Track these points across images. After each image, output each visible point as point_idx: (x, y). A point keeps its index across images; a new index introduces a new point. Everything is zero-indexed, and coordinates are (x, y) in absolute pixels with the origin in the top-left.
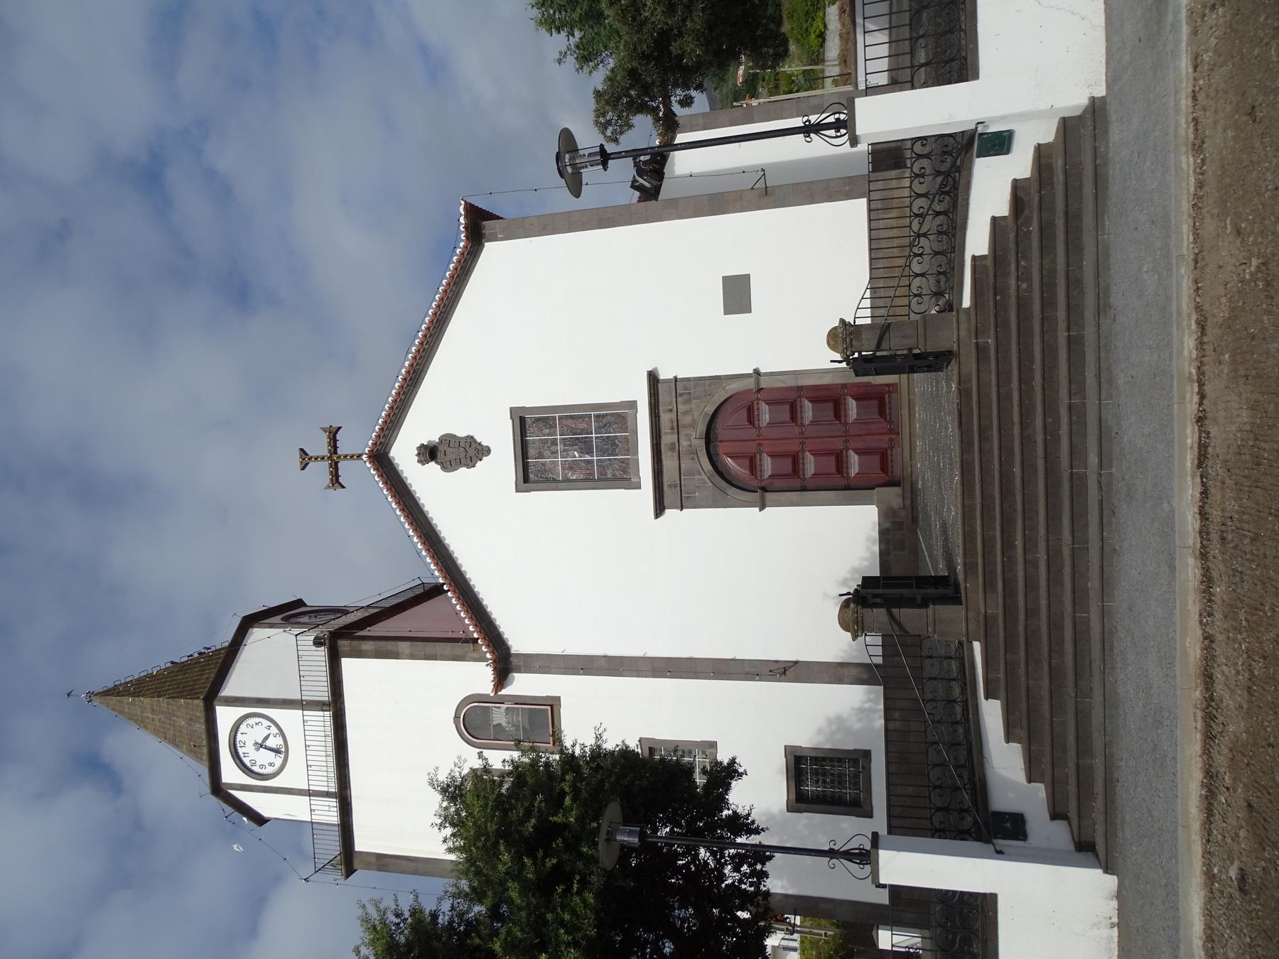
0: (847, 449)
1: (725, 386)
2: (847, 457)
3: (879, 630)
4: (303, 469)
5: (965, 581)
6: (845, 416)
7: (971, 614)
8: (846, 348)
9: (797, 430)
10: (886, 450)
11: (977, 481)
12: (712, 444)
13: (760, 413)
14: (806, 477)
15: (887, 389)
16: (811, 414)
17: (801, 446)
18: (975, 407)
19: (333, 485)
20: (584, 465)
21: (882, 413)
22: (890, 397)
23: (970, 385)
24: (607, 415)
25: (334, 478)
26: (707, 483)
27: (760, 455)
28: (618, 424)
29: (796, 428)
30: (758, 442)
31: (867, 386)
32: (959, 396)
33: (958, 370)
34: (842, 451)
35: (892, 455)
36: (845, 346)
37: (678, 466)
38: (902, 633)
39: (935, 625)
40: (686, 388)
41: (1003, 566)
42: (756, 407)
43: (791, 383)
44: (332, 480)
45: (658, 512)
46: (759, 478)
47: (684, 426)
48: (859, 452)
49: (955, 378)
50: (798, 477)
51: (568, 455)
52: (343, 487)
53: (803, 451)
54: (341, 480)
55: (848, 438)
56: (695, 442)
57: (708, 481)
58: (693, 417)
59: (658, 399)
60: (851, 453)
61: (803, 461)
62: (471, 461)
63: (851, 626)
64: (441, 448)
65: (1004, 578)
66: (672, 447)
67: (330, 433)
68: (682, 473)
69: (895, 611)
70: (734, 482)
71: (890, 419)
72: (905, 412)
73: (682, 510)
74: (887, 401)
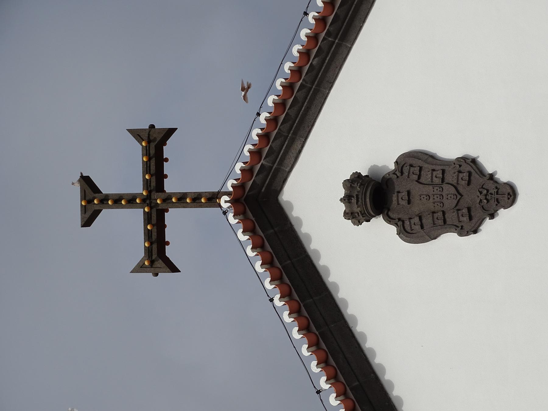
4: (87, 223)
19: (152, 262)
25: (155, 246)
44: (149, 252)
52: (174, 269)
54: (169, 252)
62: (471, 218)
64: (401, 186)
67: (149, 142)
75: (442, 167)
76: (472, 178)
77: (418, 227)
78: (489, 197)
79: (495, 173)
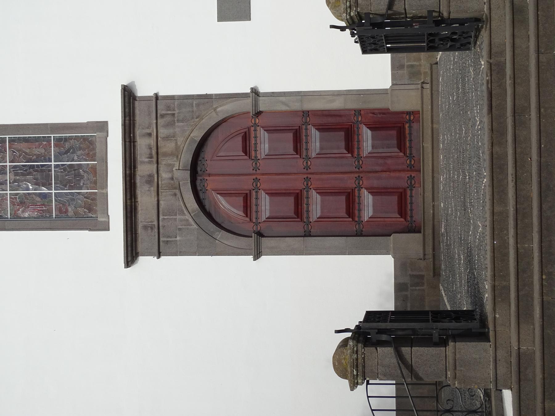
0: (360, 188)
1: (217, 107)
2: (359, 197)
3: (387, 376)
5: (494, 310)
6: (359, 148)
7: (500, 353)
8: (350, 7)
9: (300, 163)
10: (405, 190)
11: (510, 178)
12: (199, 178)
13: (258, 142)
14: (311, 220)
15: (407, 117)
16: (318, 144)
17: (305, 183)
18: (509, 82)
20: (38, 199)
21: (401, 146)
22: (410, 127)
23: (503, 59)
24: (71, 138)
26: (191, 225)
27: (257, 192)
28: (84, 150)
29: (300, 161)
30: (254, 177)
31: (384, 114)
32: (489, 72)
33: (488, 38)
34: (353, 190)
35: (411, 196)
36: (348, 4)
37: (156, 202)
38: (415, 381)
39: (455, 369)
40: (168, 108)
41: (542, 285)
42: (253, 135)
43: (296, 106)
45: (129, 259)
46: (254, 220)
47: (166, 155)
48: (374, 192)
49: (485, 53)
50: (302, 220)
51: (19, 186)
53: (308, 188)
55: (361, 175)
56: (178, 174)
57: (193, 223)
58: (176, 143)
59: (134, 120)
60: (365, 192)
61: (308, 201)
63: (349, 370)
65: (543, 301)
66: (149, 180)
68: (161, 213)
69: (405, 350)
70: (223, 225)
71: (411, 154)
72: (428, 145)
73: (159, 257)
74: (407, 131)
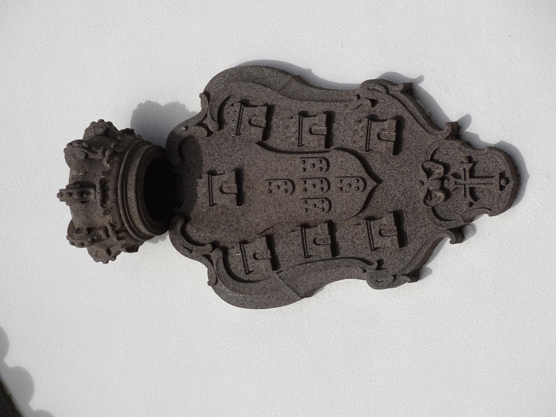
62: (402, 241)
75: (327, 107)
76: (406, 134)
77: (264, 265)
78: (450, 185)
79: (467, 119)
